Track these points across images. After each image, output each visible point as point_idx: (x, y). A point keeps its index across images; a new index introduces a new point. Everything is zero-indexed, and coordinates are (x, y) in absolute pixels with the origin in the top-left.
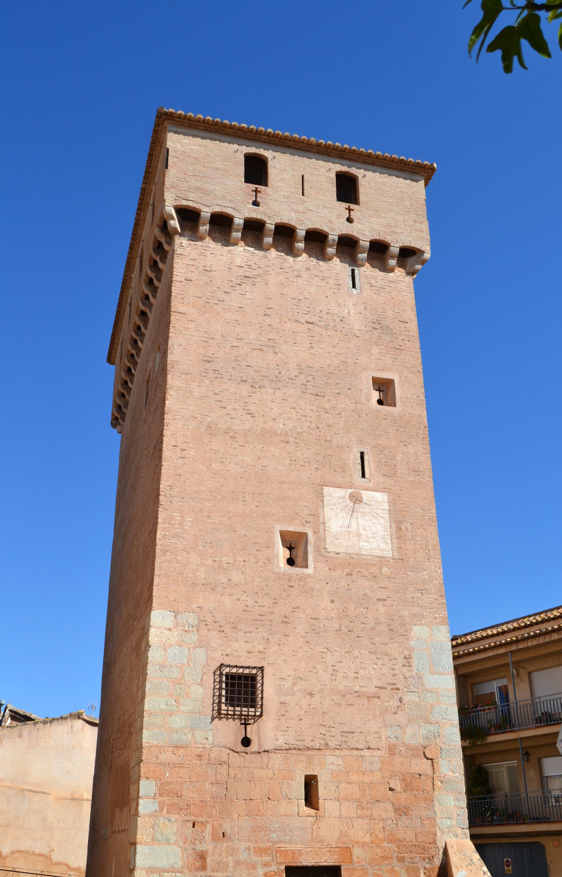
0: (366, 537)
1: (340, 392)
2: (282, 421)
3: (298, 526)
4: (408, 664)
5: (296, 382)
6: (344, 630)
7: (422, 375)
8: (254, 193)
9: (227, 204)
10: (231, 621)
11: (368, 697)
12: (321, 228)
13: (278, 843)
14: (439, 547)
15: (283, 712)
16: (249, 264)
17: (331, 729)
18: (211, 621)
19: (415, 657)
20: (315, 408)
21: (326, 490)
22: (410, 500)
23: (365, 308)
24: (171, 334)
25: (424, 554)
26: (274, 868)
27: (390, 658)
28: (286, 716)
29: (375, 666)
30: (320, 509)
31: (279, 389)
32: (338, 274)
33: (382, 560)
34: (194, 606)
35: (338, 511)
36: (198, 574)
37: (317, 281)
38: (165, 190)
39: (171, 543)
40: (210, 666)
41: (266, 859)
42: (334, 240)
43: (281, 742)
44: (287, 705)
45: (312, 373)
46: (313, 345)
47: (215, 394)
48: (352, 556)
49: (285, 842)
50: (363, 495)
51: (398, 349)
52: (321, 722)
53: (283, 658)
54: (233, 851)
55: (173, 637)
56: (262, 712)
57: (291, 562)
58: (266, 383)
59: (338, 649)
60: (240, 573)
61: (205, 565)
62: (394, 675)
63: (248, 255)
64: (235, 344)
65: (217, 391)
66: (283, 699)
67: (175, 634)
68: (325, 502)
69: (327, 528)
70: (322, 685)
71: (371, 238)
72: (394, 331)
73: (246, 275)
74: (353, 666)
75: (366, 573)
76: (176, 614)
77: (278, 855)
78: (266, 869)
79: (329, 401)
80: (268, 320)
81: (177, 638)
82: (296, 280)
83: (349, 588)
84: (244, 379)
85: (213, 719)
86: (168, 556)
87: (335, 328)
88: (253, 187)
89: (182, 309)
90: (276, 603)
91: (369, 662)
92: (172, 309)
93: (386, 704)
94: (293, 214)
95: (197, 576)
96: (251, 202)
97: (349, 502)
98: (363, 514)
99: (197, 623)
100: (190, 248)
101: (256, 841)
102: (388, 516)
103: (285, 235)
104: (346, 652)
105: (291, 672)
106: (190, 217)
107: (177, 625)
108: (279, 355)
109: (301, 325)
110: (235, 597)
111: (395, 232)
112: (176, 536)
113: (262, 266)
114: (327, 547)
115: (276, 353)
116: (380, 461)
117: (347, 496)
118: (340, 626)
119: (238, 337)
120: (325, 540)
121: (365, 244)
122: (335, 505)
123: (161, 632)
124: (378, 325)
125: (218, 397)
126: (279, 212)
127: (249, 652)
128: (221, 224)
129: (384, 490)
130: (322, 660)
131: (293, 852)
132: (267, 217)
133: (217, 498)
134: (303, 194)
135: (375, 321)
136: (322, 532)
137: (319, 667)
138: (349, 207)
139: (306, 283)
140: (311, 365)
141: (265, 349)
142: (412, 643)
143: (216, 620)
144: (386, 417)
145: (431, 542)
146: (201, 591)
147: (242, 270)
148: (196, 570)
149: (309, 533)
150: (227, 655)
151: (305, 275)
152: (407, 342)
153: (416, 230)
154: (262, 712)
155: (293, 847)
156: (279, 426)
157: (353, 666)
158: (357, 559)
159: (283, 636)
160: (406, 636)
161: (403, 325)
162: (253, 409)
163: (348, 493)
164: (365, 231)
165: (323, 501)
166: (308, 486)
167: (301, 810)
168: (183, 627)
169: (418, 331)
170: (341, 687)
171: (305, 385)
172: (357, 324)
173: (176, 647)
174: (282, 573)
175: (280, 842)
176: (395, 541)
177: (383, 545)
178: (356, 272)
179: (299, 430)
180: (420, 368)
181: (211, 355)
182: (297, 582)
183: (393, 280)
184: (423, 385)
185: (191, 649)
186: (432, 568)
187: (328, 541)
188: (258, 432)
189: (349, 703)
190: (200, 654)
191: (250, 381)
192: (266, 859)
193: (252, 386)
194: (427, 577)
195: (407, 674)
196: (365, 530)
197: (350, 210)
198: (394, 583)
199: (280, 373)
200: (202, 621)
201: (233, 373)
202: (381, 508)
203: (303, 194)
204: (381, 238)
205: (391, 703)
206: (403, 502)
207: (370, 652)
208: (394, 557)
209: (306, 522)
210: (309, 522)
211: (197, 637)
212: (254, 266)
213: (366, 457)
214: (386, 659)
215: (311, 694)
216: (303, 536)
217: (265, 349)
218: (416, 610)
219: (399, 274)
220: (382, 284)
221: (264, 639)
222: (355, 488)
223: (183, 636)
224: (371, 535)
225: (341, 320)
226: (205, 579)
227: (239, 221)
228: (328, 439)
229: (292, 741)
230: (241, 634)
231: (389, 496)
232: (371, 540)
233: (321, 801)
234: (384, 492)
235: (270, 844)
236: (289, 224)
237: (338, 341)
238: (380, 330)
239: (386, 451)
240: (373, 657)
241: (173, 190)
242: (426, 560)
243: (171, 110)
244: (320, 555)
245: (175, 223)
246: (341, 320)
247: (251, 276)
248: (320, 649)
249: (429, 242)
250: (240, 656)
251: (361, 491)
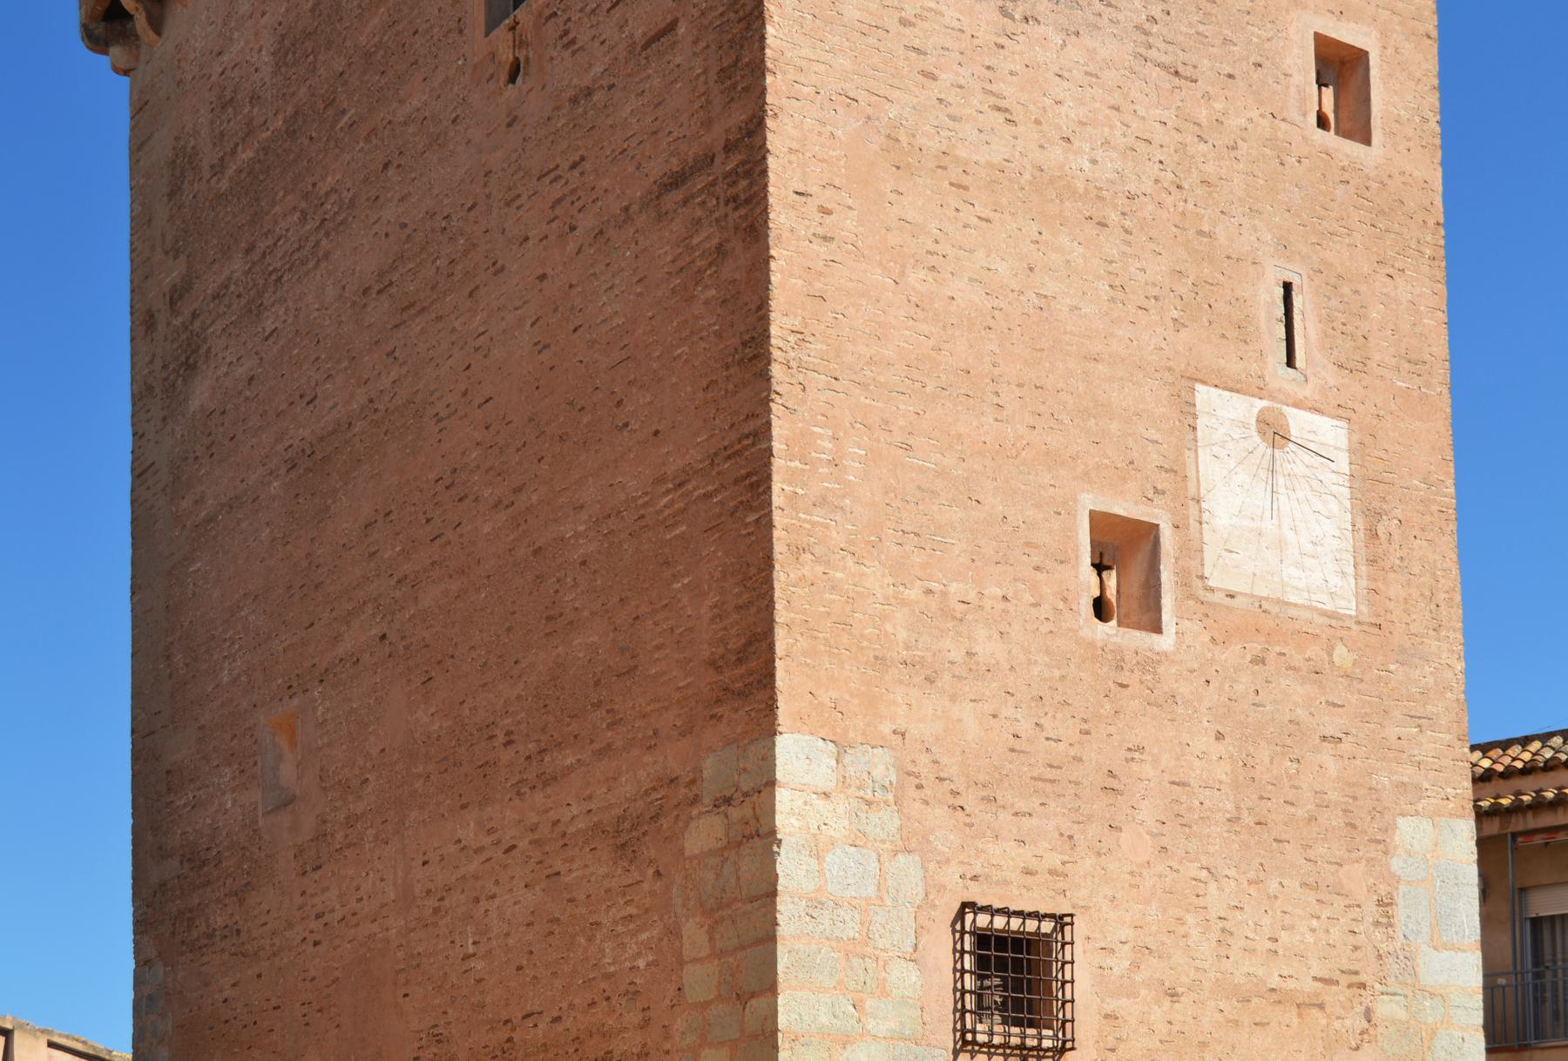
3: (1136, 503)
4: (1384, 920)
6: (1248, 819)
10: (981, 778)
11: (1298, 1006)
14: (1458, 598)
15: (1111, 1042)
18: (932, 777)
19: (1400, 902)
22: (1398, 448)
25: (1427, 614)
27: (1347, 902)
28: (1119, 1052)
29: (1314, 923)
30: (1187, 453)
33: (1334, 623)
34: (886, 728)
35: (1232, 463)
36: (889, 628)
39: (813, 524)
40: (934, 906)
44: (1120, 1021)
48: (1265, 606)
53: (1110, 893)
55: (837, 818)
60: (996, 636)
61: (905, 603)
62: (1356, 948)
66: (1111, 1005)
67: (840, 810)
68: (1199, 434)
69: (1205, 516)
70: (1197, 969)
74: (1266, 921)
76: (842, 748)
81: (846, 822)
86: (809, 568)
90: (1088, 733)
91: (1300, 912)
93: (1337, 1024)
95: (886, 634)
97: (1257, 439)
99: (894, 778)
102: (1347, 492)
104: (1250, 882)
105: (1127, 933)
107: (844, 781)
110: (987, 708)
112: (821, 502)
117: (1253, 421)
123: (806, 803)
127: (1028, 872)
129: (1340, 411)
133: (929, 389)
136: (1193, 523)
142: (1396, 864)
143: (942, 775)
145: (1442, 581)
146: (900, 682)
148: (884, 618)
150: (975, 878)
157: (1266, 921)
158: (1277, 616)
160: (1382, 843)
163: (1256, 411)
165: (1194, 429)
166: (1158, 375)
168: (859, 788)
170: (1239, 979)
173: (847, 848)
174: (1100, 644)
176: (1363, 569)
177: (1335, 580)
182: (1137, 673)
185: (885, 857)
186: (1445, 655)
187: (1209, 555)
189: (1258, 1020)
190: (908, 871)
194: (1430, 680)
195: (1384, 947)
196: (1294, 529)
198: (1359, 692)
200: (908, 774)
205: (1348, 1022)
206: (1382, 454)
207: (1304, 885)
208: (1361, 618)
209: (1156, 491)
210: (1163, 493)
211: (897, 822)
214: (1340, 902)
215: (1173, 995)
216: (1145, 535)
218: (1407, 774)
221: (1062, 835)
222: (1272, 398)
223: (863, 816)
224: (1309, 548)
226: (907, 648)
230: (1005, 816)
231: (1351, 431)
234: (1340, 417)
240: (1311, 897)
242: (1431, 633)
248: (1192, 870)
250: (1006, 882)
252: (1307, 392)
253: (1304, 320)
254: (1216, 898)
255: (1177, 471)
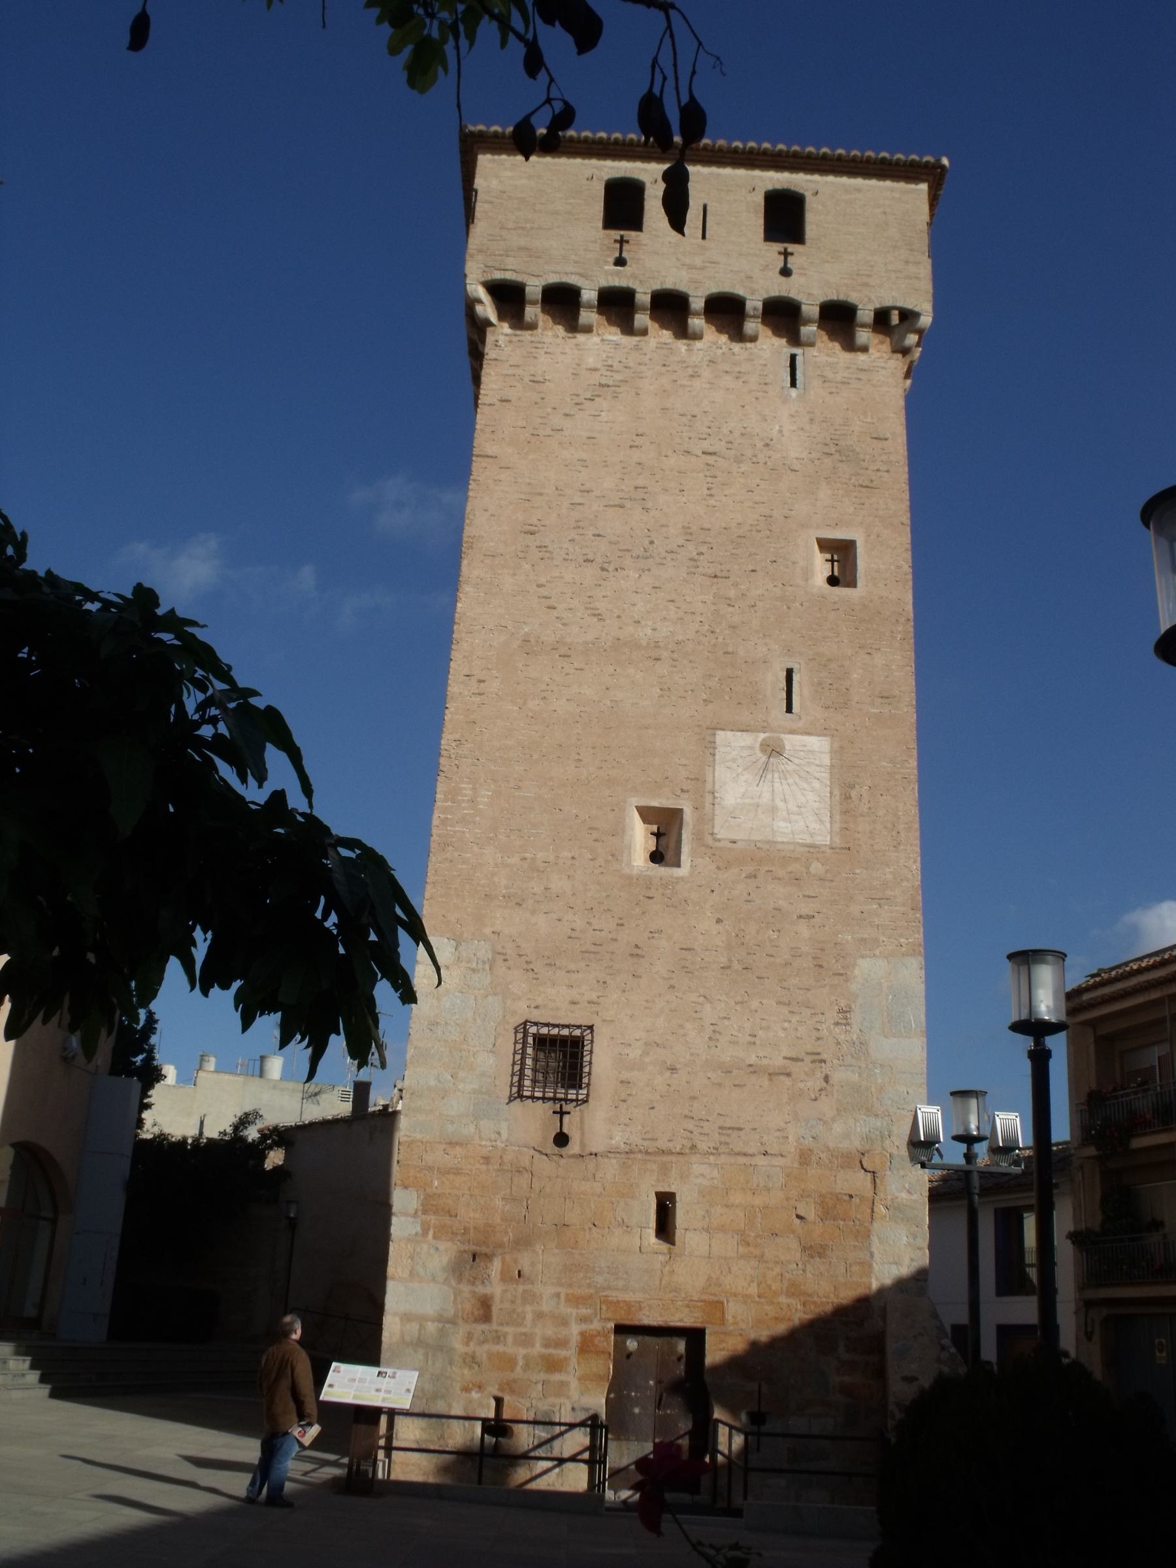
0: (785, 813)
1: (757, 568)
2: (650, 623)
5: (679, 557)
6: (736, 966)
7: (908, 529)
8: (618, 245)
9: (570, 269)
12: (731, 291)
13: (604, 1289)
16: (610, 363)
17: (702, 1124)
20: (709, 598)
21: (721, 736)
23: (812, 420)
24: (470, 494)
26: (596, 1325)
31: (649, 570)
32: (765, 365)
35: (740, 770)
37: (728, 381)
38: (468, 257)
41: (584, 1311)
42: (755, 309)
43: (618, 1139)
45: (708, 539)
46: (712, 492)
47: (539, 586)
48: (759, 845)
49: (617, 1289)
50: (786, 743)
51: (867, 487)
52: (686, 1112)
54: (530, 1298)
56: (588, 1095)
57: (657, 857)
58: (628, 561)
59: (724, 998)
63: (607, 348)
64: (577, 500)
65: (543, 580)
66: (625, 1075)
68: (717, 757)
69: (717, 801)
71: (822, 299)
72: (861, 456)
73: (603, 381)
75: (781, 873)
77: (604, 1307)
78: (584, 1327)
79: (735, 585)
80: (636, 455)
82: (689, 383)
83: (750, 898)
84: (590, 557)
85: (511, 1099)
87: (755, 460)
88: (616, 234)
89: (490, 449)
92: (476, 451)
94: (684, 274)
96: (611, 260)
97: (760, 754)
98: (784, 775)
100: (510, 348)
101: (570, 1286)
103: (671, 307)
106: (508, 296)
108: (652, 513)
109: (694, 459)
111: (866, 285)
113: (631, 364)
114: (716, 831)
115: (647, 510)
116: (820, 684)
117: (758, 745)
118: (730, 961)
119: (583, 488)
120: (713, 819)
121: (811, 309)
122: (734, 760)
124: (836, 451)
125: (543, 592)
126: (658, 272)
128: (562, 301)
130: (694, 1015)
131: (628, 1305)
132: (638, 282)
134: (704, 237)
135: (828, 441)
136: (708, 806)
137: (688, 1025)
138: (786, 249)
139: (707, 386)
140: (707, 526)
141: (628, 504)
144: (836, 606)
147: (596, 375)
149: (685, 809)
151: (706, 373)
152: (885, 474)
153: (908, 277)
154: (588, 1095)
155: (629, 1297)
156: (645, 633)
159: (631, 977)
161: (879, 444)
162: (601, 606)
164: (810, 288)
167: (645, 1243)
169: (906, 454)
171: (695, 560)
172: (795, 449)
175: (609, 1288)
177: (814, 826)
178: (799, 360)
179: (680, 638)
180: (906, 518)
181: (535, 522)
182: (661, 890)
183: (865, 367)
184: (909, 546)
187: (718, 821)
188: (609, 644)
191: (599, 559)
192: (584, 1311)
193: (603, 569)
196: (785, 801)
197: (786, 254)
199: (652, 542)
201: (571, 550)
202: (817, 762)
203: (704, 237)
204: (842, 297)
212: (616, 365)
213: (796, 678)
215: (673, 1069)
217: (628, 504)
219: (878, 355)
220: (846, 375)
222: (772, 731)
224: (795, 809)
225: (767, 445)
227: (589, 295)
228: (730, 649)
229: (636, 1140)
232: (793, 817)
233: (679, 1233)
234: (825, 735)
235: (592, 1291)
236: (677, 291)
237: (758, 481)
238: (837, 456)
239: (833, 666)
241: (480, 257)
243: (481, 127)
244: (704, 845)
245: (487, 309)
246: (767, 445)
247: (611, 383)
248: (693, 997)
249: (930, 297)
251: (782, 736)
252: (801, 724)
253: (800, 687)
254: (709, 1013)
255: (698, 780)
